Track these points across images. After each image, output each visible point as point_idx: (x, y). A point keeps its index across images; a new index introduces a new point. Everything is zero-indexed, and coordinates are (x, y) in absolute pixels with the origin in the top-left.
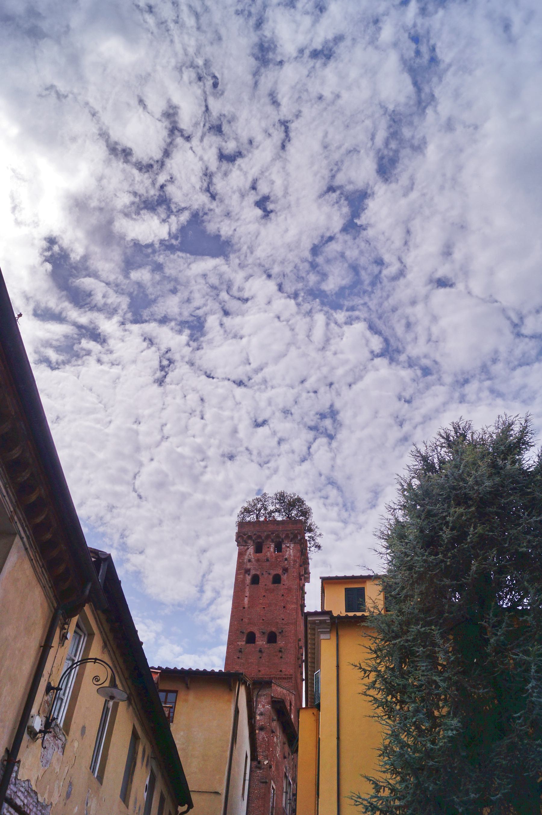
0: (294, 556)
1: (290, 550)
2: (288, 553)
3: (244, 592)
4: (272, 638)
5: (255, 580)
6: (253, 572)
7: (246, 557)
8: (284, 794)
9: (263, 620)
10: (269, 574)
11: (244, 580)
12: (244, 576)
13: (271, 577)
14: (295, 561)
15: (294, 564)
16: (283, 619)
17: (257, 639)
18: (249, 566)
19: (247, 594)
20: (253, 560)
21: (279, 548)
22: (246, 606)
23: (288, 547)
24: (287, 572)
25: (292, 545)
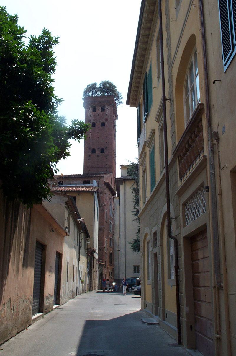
0: (111, 113)
1: (108, 110)
2: (107, 112)
4: (102, 151)
6: (92, 121)
8: (110, 211)
10: (100, 122)
13: (101, 123)
14: (111, 115)
20: (92, 115)
21: (103, 110)
23: (107, 109)
24: (107, 121)
25: (109, 108)
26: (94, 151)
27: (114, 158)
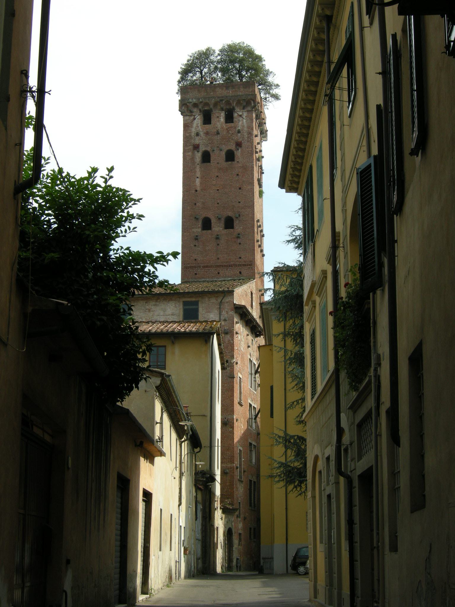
3: (195, 172)
4: (229, 223)
5: (206, 157)
6: (202, 148)
7: (193, 130)
9: (218, 204)
11: (193, 158)
12: (193, 153)
13: (223, 153)
15: (248, 137)
16: (239, 202)
17: (212, 225)
18: (197, 141)
19: (198, 174)
20: (201, 134)
22: (198, 189)
26: (207, 224)
27: (258, 241)
